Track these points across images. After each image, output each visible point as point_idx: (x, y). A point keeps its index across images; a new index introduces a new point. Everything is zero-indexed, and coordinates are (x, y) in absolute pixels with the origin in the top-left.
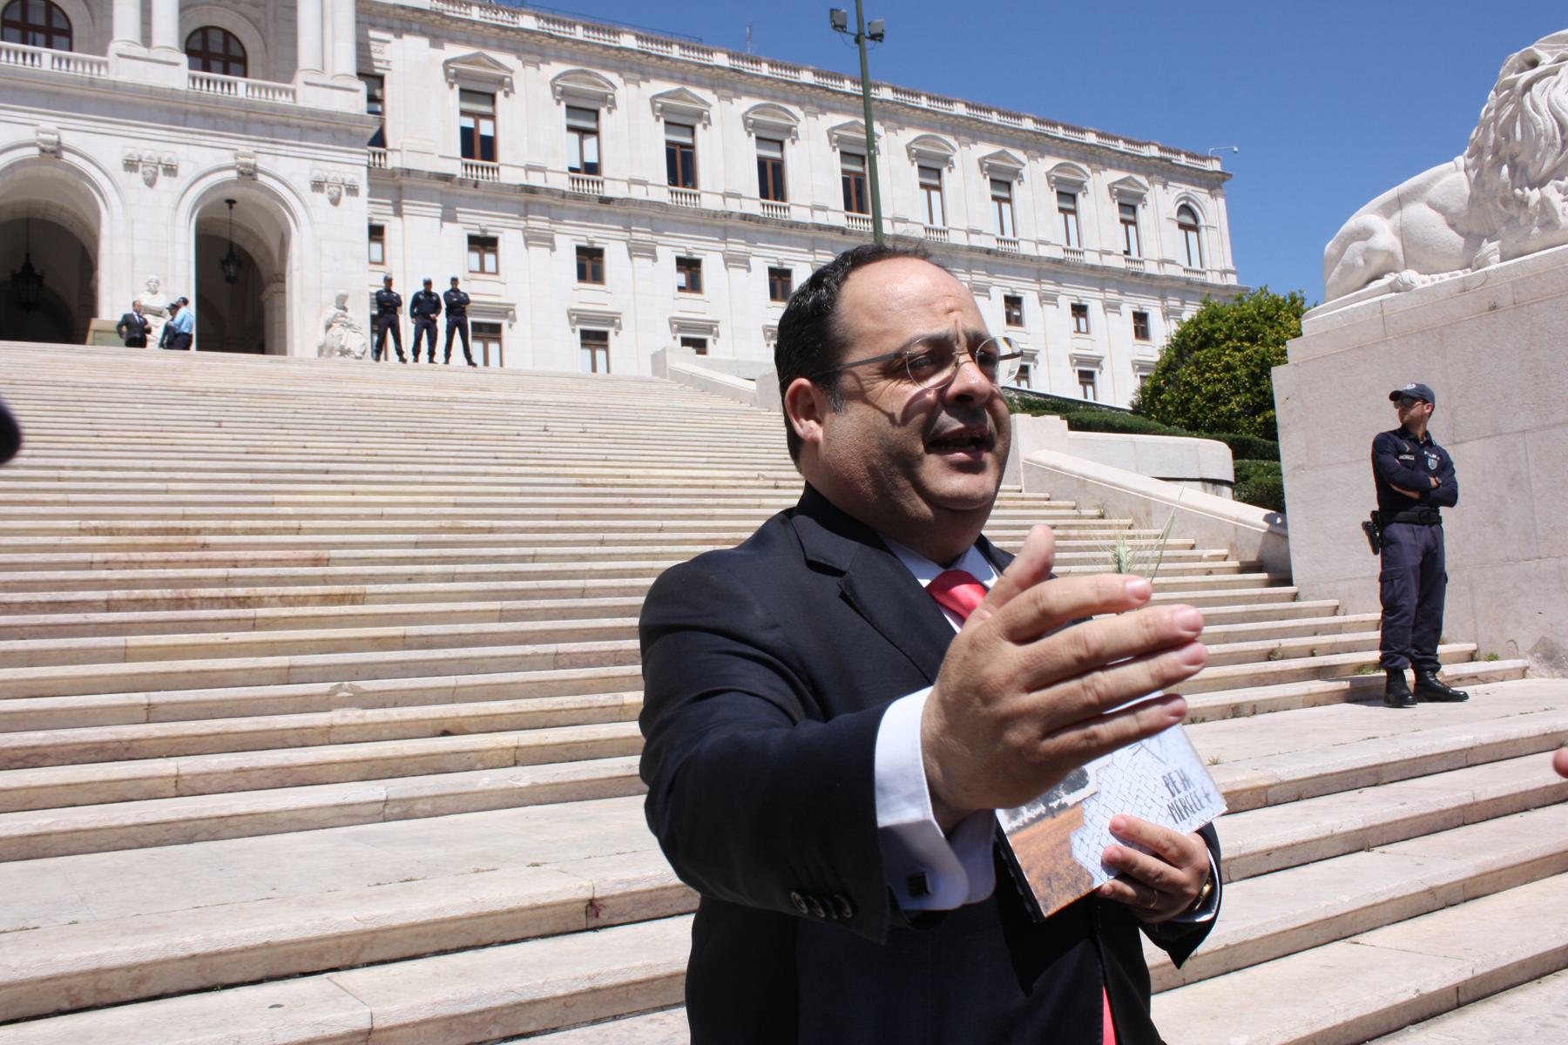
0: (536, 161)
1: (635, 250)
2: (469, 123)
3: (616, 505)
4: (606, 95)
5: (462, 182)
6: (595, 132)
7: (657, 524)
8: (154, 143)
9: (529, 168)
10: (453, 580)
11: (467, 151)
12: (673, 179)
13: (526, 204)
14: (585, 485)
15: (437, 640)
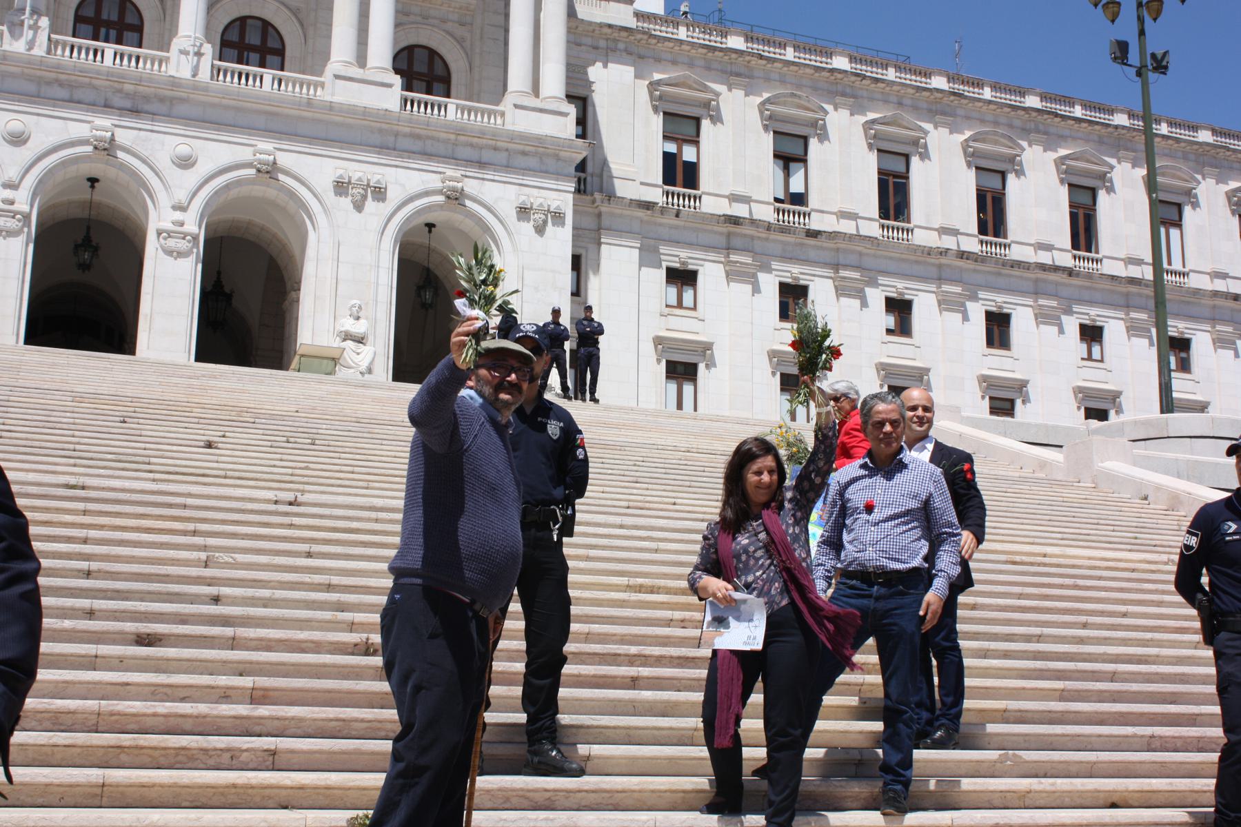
0: (740, 190)
1: (841, 291)
2: (672, 148)
3: (1062, 586)
4: (817, 120)
5: (663, 210)
6: (803, 160)
7: (1123, 608)
8: (363, 168)
9: (734, 198)
10: (985, 657)
11: (669, 178)
12: (884, 213)
13: (729, 235)
14: (1014, 563)
15: (1029, 715)
